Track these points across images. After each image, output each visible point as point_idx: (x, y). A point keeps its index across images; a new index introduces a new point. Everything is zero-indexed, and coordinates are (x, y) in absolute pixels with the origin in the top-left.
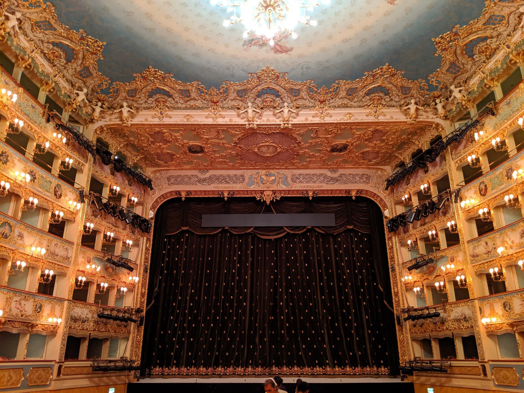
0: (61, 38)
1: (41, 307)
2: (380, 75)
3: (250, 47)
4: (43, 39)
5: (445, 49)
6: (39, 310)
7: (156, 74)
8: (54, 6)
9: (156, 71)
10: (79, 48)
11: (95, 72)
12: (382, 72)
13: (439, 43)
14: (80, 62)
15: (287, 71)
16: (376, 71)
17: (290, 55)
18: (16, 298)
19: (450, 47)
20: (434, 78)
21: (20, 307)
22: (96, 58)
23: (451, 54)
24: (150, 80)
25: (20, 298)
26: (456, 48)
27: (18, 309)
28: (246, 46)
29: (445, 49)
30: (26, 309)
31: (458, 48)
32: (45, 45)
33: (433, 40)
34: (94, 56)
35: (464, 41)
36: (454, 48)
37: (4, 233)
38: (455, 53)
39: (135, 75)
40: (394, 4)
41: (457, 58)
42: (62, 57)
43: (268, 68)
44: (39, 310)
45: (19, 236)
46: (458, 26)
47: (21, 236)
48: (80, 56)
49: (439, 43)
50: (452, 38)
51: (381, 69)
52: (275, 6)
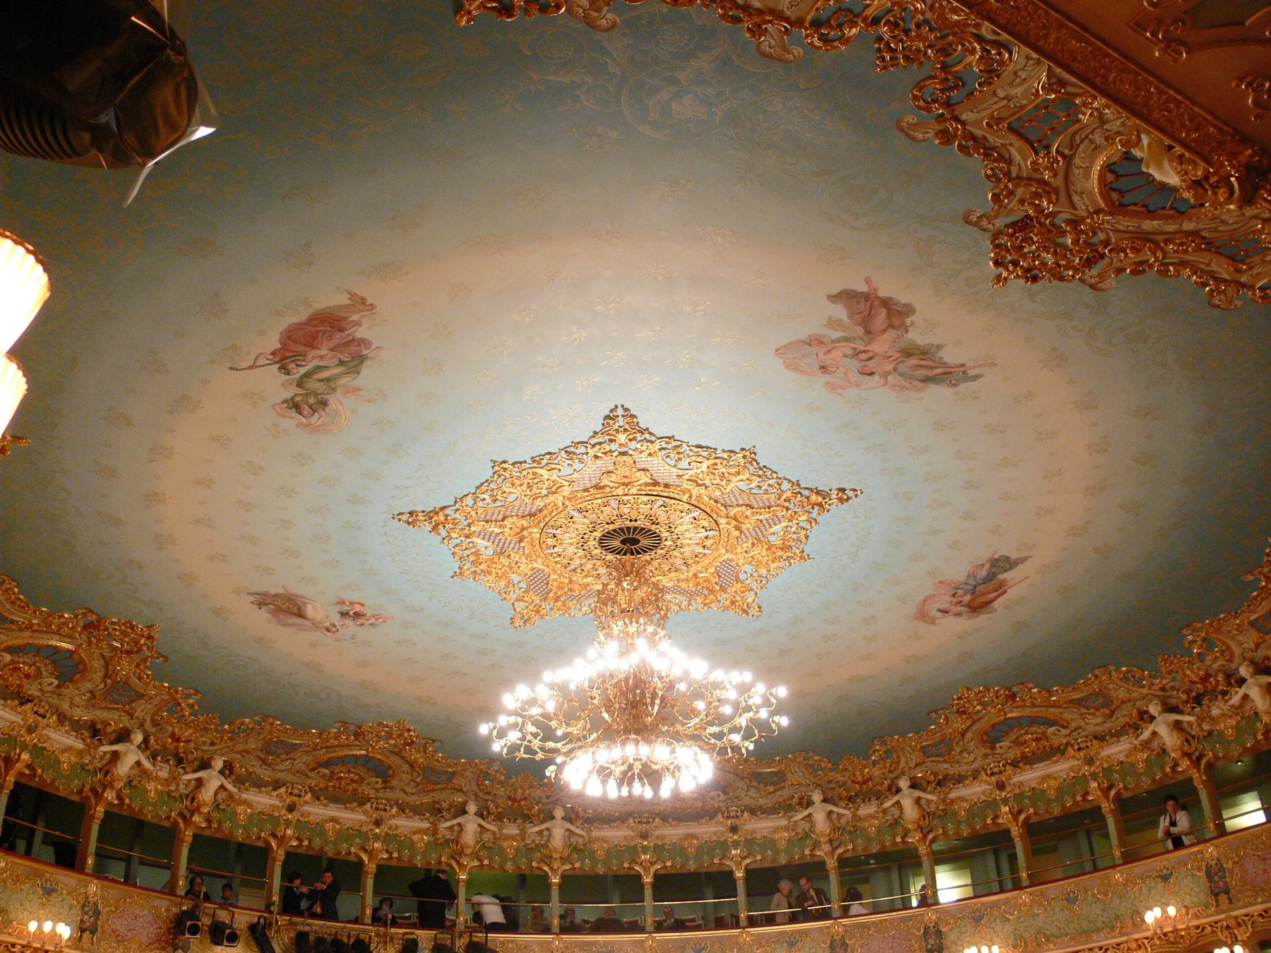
17: (867, 281)
40: (353, 296)
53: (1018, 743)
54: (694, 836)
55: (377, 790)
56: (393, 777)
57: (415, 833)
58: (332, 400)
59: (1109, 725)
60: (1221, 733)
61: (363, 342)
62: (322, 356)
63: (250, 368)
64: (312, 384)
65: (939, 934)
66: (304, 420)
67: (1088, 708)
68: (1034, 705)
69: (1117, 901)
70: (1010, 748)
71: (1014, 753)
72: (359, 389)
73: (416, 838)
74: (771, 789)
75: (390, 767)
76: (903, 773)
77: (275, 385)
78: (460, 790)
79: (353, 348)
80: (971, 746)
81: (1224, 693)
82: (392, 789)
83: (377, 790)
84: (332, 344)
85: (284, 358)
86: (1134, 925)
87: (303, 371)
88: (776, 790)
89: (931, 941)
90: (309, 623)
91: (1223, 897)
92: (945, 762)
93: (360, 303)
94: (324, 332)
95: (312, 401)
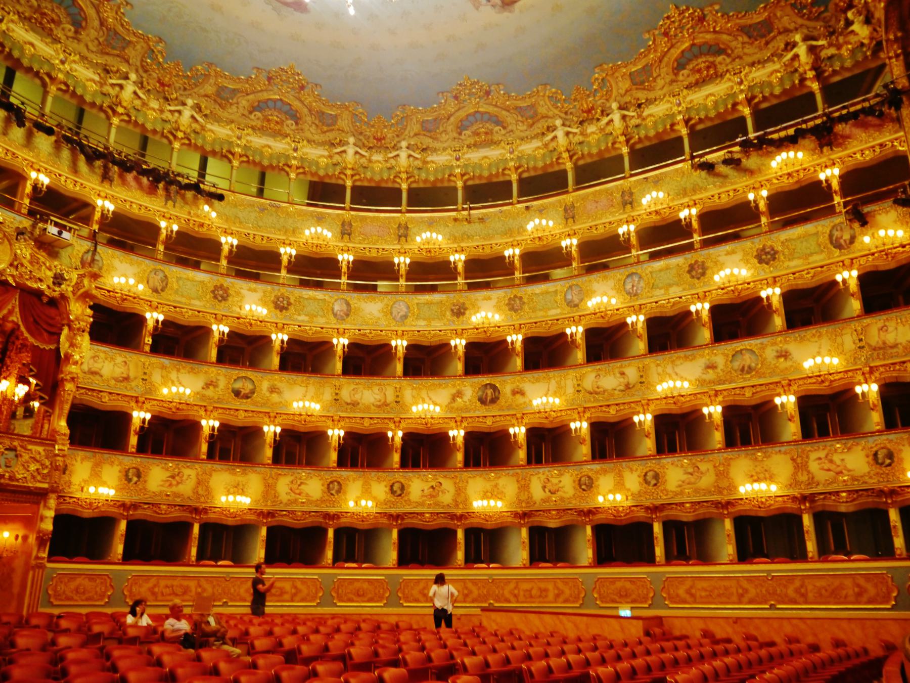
0: (666, 59)
1: (890, 455)
4: (668, 80)
6: (888, 461)
8: (601, 65)
18: (813, 456)
21: (833, 467)
25: (825, 452)
27: (829, 470)
30: (849, 466)
32: (681, 78)
37: (743, 367)
42: (711, 59)
44: (888, 461)
45: (778, 357)
47: (785, 355)
53: (476, 134)
54: (270, 147)
55: (68, 37)
56: (84, 29)
57: (88, 80)
59: (528, 133)
60: (589, 142)
65: (407, 228)
67: (522, 116)
68: (496, 106)
69: (511, 221)
70: (469, 136)
71: (471, 141)
73: (89, 84)
74: (325, 128)
75: (86, 19)
76: (404, 139)
78: (127, 61)
80: (449, 128)
81: (598, 120)
82: (79, 40)
83: (68, 37)
86: (519, 233)
88: (327, 131)
89: (402, 231)
91: (571, 220)
92: (431, 137)
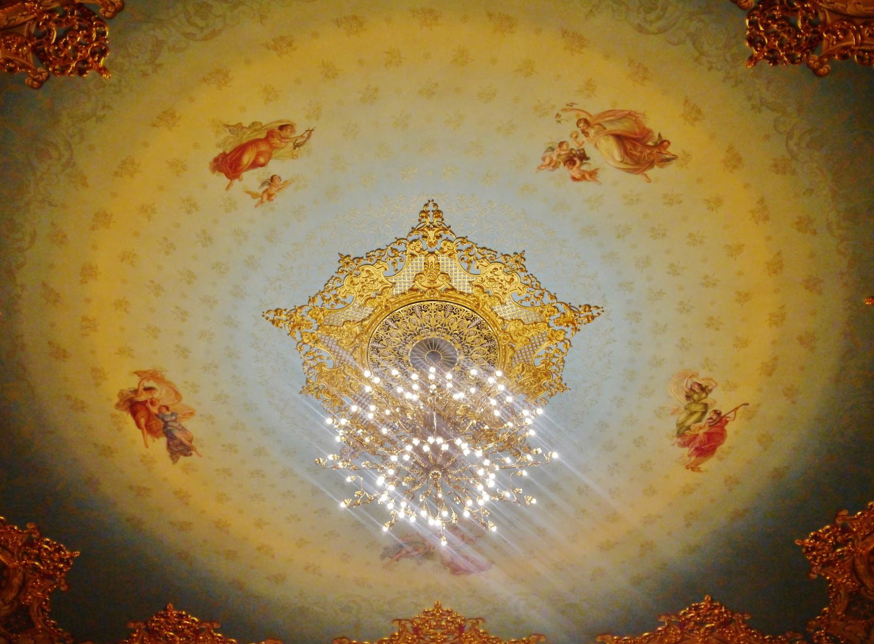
2: (696, 622)
3: (397, 560)
5: (830, 563)
7: (180, 623)
9: (180, 616)
10: (16, 563)
11: (40, 619)
12: (698, 615)
13: (813, 549)
14: (12, 595)
15: (482, 614)
16: (685, 614)
19: (840, 557)
20: (820, 629)
22: (51, 586)
23: (844, 573)
24: (166, 637)
26: (853, 560)
28: (388, 560)
29: (830, 563)
31: (858, 561)
33: (798, 542)
34: (48, 582)
35: (868, 545)
36: (848, 560)
38: (854, 571)
39: (132, 625)
40: (699, 470)
41: (860, 580)
43: (438, 607)
46: (844, 513)
48: (16, 581)
49: (813, 549)
50: (839, 538)
51: (697, 608)
52: (445, 466)
58: (685, 402)
61: (684, 445)
62: (701, 429)
63: (737, 409)
64: (699, 408)
66: (695, 380)
72: (672, 414)
77: (720, 400)
79: (687, 439)
84: (698, 440)
85: (720, 421)
87: (708, 416)
90: (610, 128)
93: (694, 467)
94: (705, 444)
95: (696, 396)
